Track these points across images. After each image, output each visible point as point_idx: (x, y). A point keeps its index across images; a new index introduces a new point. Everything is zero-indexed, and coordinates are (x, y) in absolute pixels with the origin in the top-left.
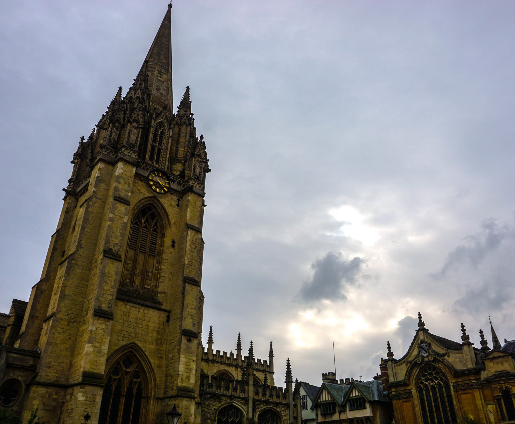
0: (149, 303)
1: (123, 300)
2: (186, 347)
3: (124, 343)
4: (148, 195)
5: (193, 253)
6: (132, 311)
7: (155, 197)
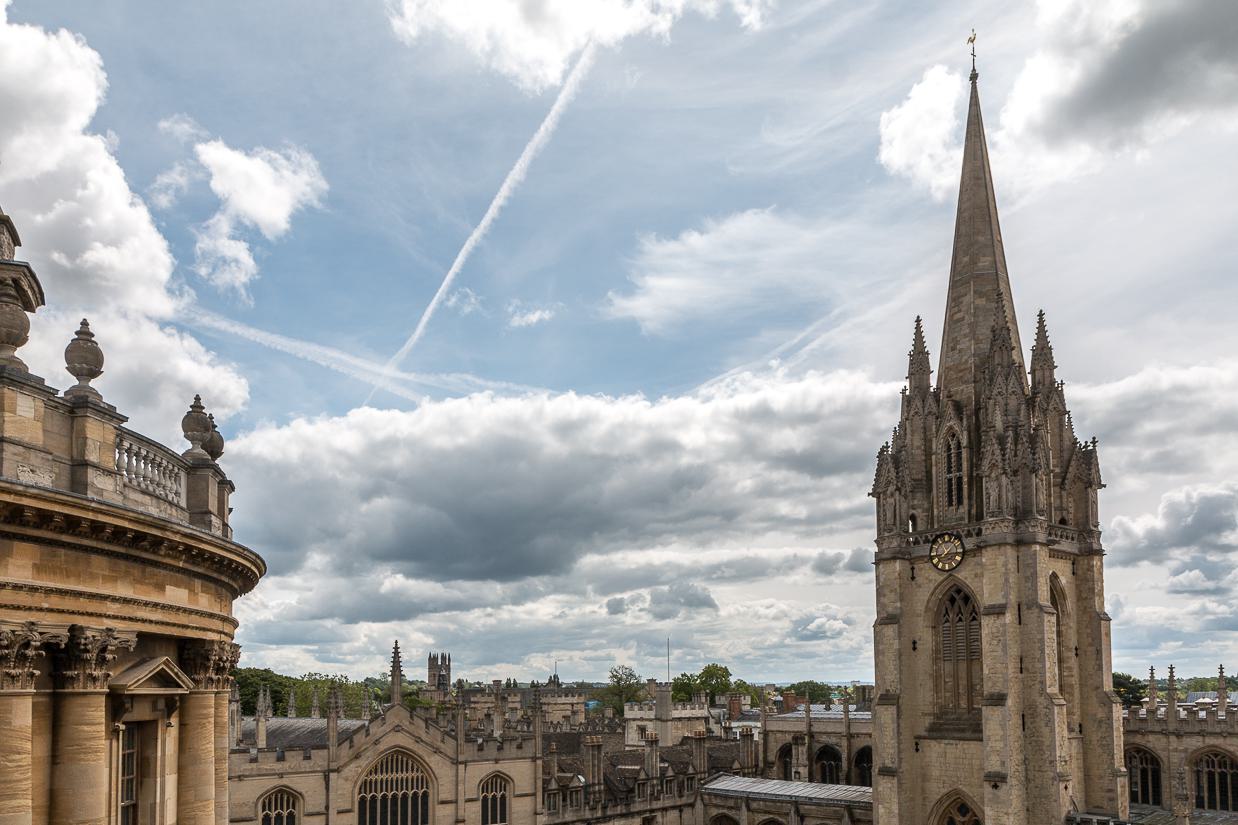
0: (968, 735)
1: (935, 739)
2: (991, 796)
3: (945, 791)
4: (942, 578)
5: (995, 654)
6: (948, 751)
7: (951, 575)
